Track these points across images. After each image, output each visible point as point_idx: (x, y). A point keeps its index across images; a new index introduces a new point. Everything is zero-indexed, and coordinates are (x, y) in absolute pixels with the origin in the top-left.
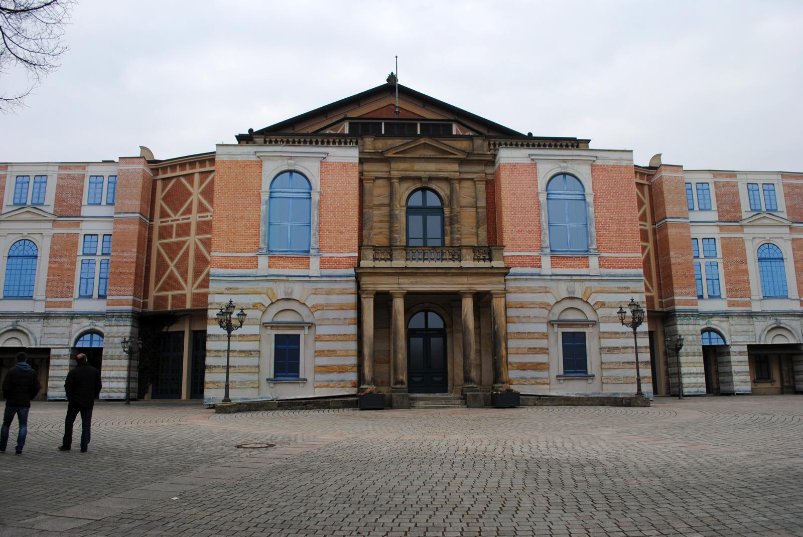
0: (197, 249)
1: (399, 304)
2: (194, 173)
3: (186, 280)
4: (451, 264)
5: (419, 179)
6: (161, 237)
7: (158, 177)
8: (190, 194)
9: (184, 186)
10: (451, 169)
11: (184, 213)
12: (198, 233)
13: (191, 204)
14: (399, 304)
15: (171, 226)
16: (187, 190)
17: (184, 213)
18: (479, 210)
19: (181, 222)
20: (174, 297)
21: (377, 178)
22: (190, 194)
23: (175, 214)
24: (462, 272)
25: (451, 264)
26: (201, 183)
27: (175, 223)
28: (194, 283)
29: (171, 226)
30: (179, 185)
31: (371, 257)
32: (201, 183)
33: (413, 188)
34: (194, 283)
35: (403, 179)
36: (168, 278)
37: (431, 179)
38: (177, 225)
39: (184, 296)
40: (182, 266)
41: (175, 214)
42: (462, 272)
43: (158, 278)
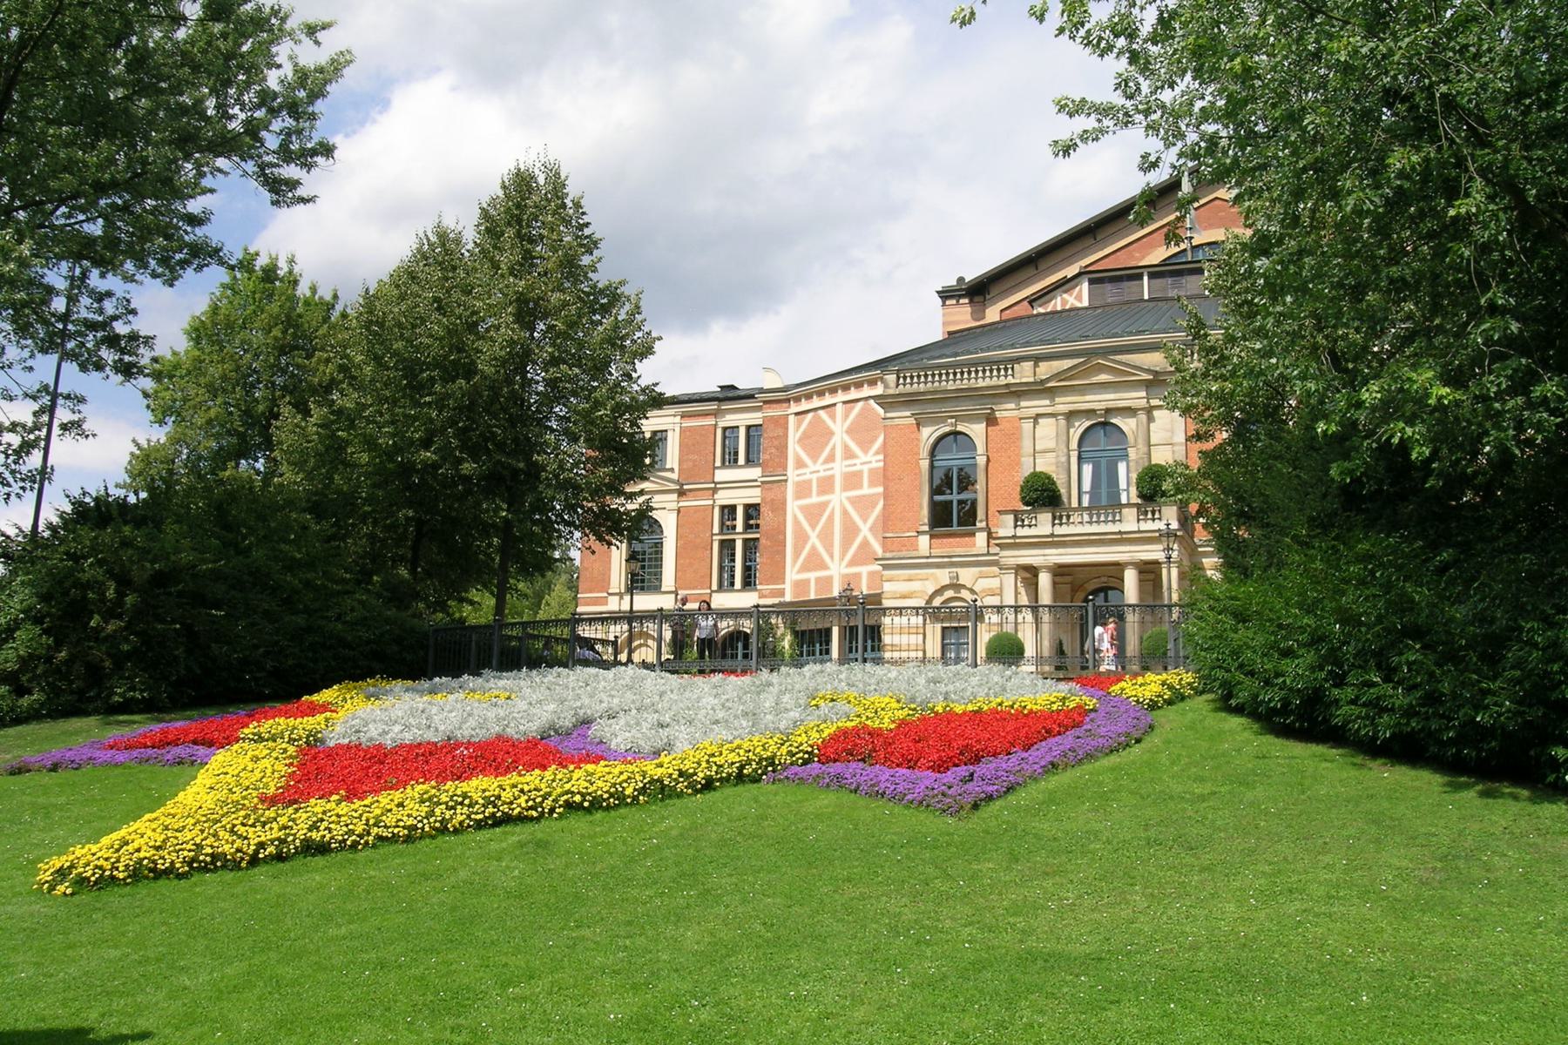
0: (845, 512)
1: (1045, 580)
2: (835, 405)
3: (832, 557)
4: (1110, 528)
5: (1094, 411)
6: (799, 495)
7: (790, 411)
8: (832, 433)
9: (824, 422)
10: (1136, 398)
11: (827, 461)
12: (846, 488)
13: (833, 448)
14: (1045, 580)
15: (810, 481)
16: (828, 428)
17: (827, 461)
18: (1176, 448)
19: (822, 474)
20: (818, 580)
21: (1038, 416)
22: (832, 433)
23: (815, 462)
24: (1122, 539)
25: (1110, 528)
26: (846, 416)
27: (814, 477)
28: (842, 559)
29: (810, 481)
30: (818, 422)
31: (1012, 523)
32: (846, 416)
33: (1088, 423)
34: (842, 559)
35: (1071, 416)
36: (809, 555)
37: (1108, 411)
38: (818, 479)
39: (829, 580)
40: (826, 537)
41: (815, 462)
42: (1122, 539)
43: (797, 555)
